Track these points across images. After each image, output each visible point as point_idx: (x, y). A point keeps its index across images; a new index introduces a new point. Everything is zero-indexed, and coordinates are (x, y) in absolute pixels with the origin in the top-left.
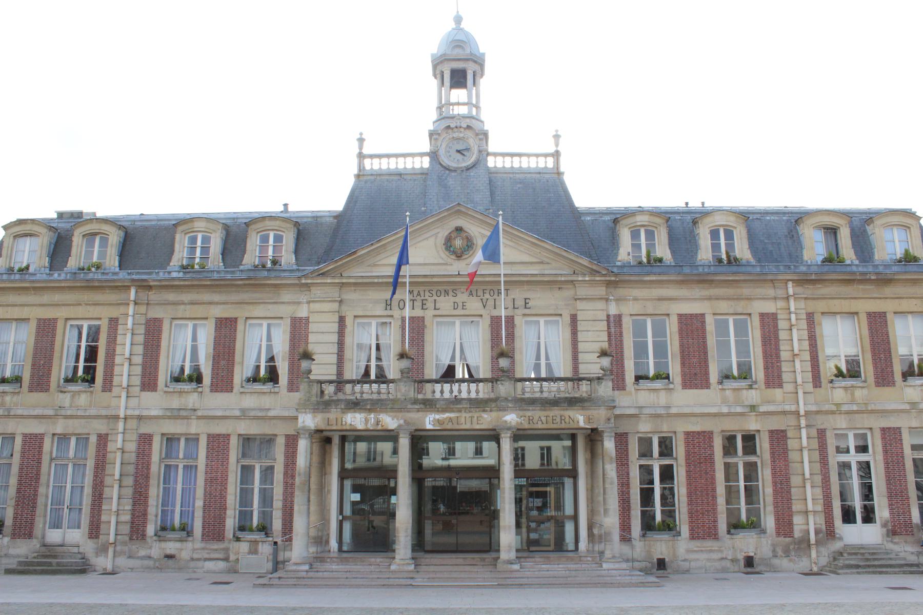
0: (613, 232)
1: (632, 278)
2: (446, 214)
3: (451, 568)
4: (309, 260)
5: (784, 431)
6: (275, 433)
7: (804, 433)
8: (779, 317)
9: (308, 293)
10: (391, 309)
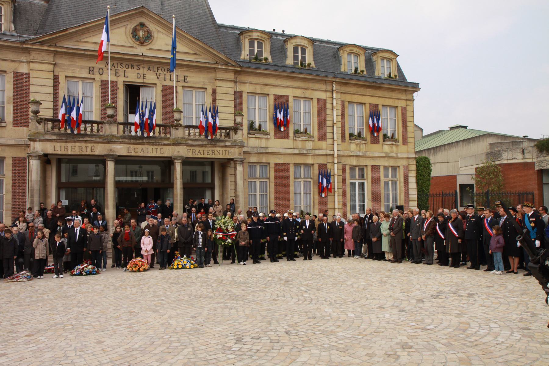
0: (238, 41)
1: (250, 70)
2: (134, 12)
4: (26, 31)
5: (326, 165)
6: (4, 156)
7: (336, 166)
8: (327, 102)
9: (28, 55)
10: (93, 74)
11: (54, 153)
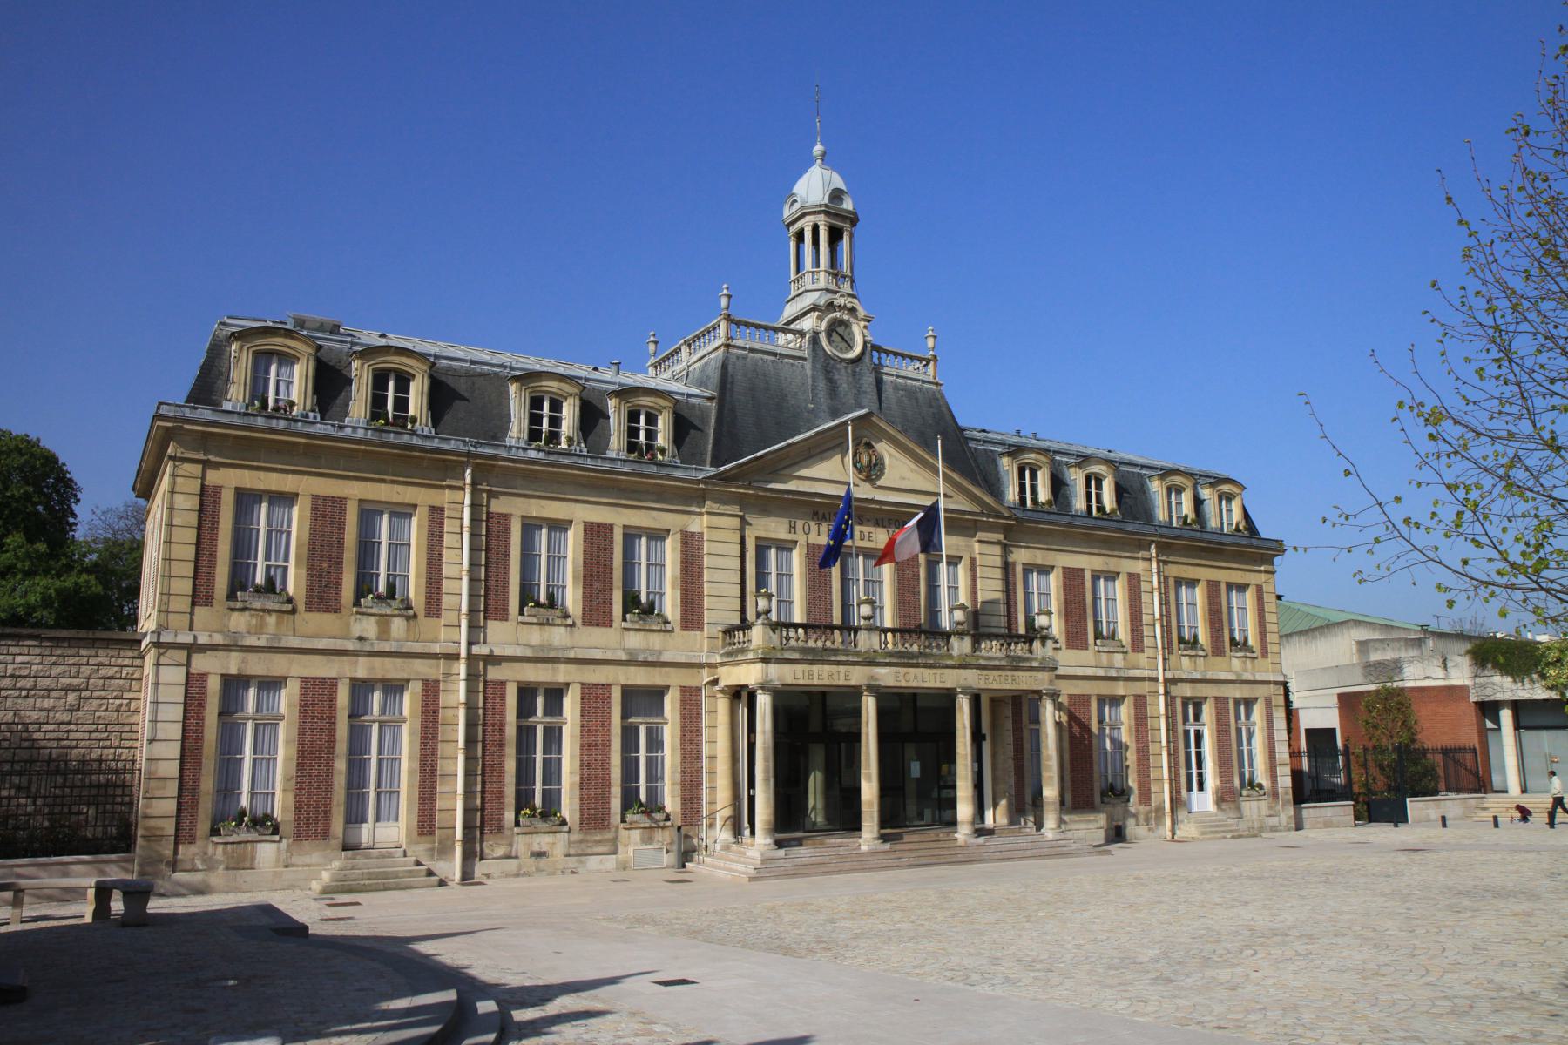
3: (917, 846)
11: (795, 682)
